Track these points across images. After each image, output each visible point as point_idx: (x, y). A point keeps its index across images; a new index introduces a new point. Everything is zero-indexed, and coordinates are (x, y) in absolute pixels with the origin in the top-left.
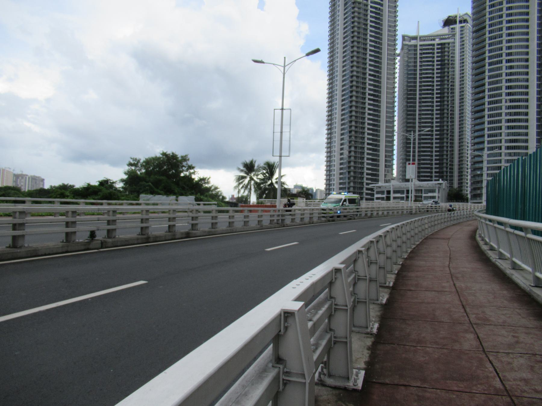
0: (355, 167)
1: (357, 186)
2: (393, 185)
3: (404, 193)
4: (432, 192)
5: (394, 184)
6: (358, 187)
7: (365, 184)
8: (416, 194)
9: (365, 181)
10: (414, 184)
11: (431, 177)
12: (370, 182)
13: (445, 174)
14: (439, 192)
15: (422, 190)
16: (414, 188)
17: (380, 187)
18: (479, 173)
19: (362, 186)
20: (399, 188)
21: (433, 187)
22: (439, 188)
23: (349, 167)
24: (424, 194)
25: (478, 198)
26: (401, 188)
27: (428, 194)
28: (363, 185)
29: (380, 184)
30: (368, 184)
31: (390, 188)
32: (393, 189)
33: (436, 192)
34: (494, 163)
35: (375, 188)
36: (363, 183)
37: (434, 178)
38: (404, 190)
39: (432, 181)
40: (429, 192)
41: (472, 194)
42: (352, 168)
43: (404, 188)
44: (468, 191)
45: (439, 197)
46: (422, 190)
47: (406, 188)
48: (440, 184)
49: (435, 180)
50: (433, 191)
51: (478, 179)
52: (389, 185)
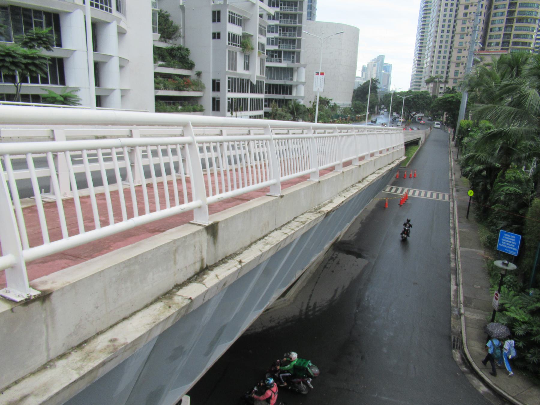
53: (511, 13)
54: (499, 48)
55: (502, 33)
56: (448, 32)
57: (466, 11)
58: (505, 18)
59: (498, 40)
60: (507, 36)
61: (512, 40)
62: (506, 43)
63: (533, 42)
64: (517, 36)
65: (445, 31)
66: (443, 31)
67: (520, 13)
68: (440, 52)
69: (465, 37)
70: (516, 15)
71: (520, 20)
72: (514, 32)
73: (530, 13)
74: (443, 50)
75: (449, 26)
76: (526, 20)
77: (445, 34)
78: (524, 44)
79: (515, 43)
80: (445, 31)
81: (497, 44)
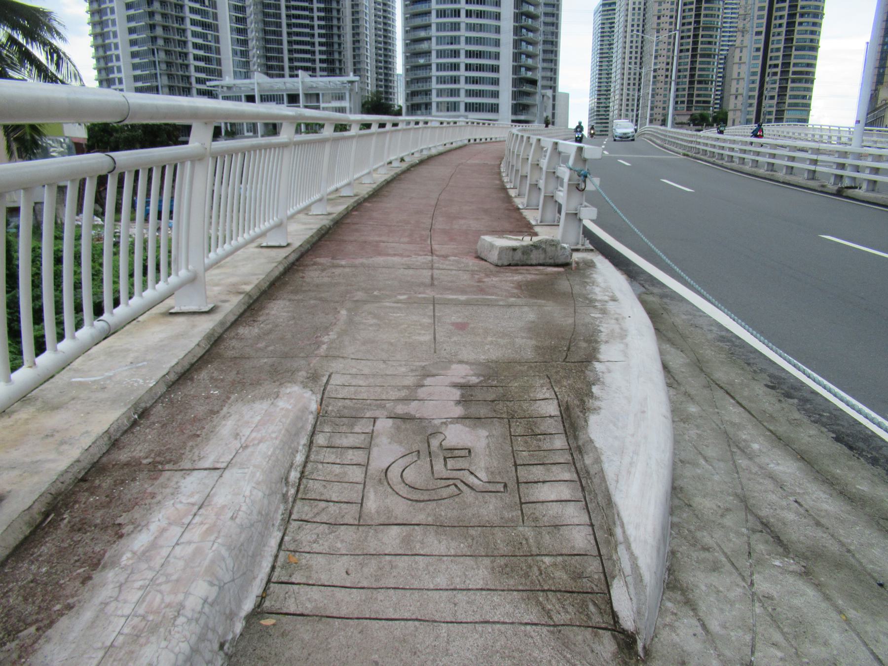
0: (167, 41)
1: (176, 84)
2: (258, 83)
3: (283, 100)
4: (339, 99)
5: (260, 81)
6: (179, 87)
7: (193, 80)
8: (307, 102)
9: (194, 74)
10: (302, 82)
11: (314, 70)
12: (203, 76)
13: (337, 65)
14: (350, 100)
15: (318, 95)
16: (303, 89)
17: (229, 88)
18: (422, 61)
19: (188, 86)
20: (268, 91)
21: (340, 89)
22: (351, 90)
23: (154, 39)
24: (323, 102)
25: (419, 112)
26: (277, 91)
27: (330, 102)
28: (191, 84)
29: (228, 79)
30: (199, 81)
31: (253, 89)
32: (259, 91)
33: (345, 99)
34: (448, 44)
35: (220, 90)
36: (188, 77)
37: (318, 73)
38: (283, 95)
39: (315, 76)
40: (333, 99)
41: (409, 104)
42: (160, 42)
43: (281, 90)
44: (400, 99)
45: (350, 108)
46: (318, 95)
47: (286, 90)
48: (352, 82)
49: (321, 76)
50: (341, 98)
51: (421, 74)
52: (251, 84)
53: (692, 76)
54: (685, 105)
55: (686, 93)
56: (634, 84)
57: (656, 74)
58: (687, 80)
59: (683, 99)
60: (691, 95)
61: (695, 99)
62: (690, 102)
63: (712, 100)
64: (698, 96)
65: (632, 84)
66: (629, 84)
67: (700, 76)
68: (627, 105)
69: (656, 97)
70: (696, 78)
71: (700, 82)
72: (696, 92)
73: (708, 76)
74: (630, 103)
75: (634, 79)
76: (706, 83)
77: (631, 87)
78: (704, 102)
79: (697, 102)
80: (632, 84)
81: (683, 102)
